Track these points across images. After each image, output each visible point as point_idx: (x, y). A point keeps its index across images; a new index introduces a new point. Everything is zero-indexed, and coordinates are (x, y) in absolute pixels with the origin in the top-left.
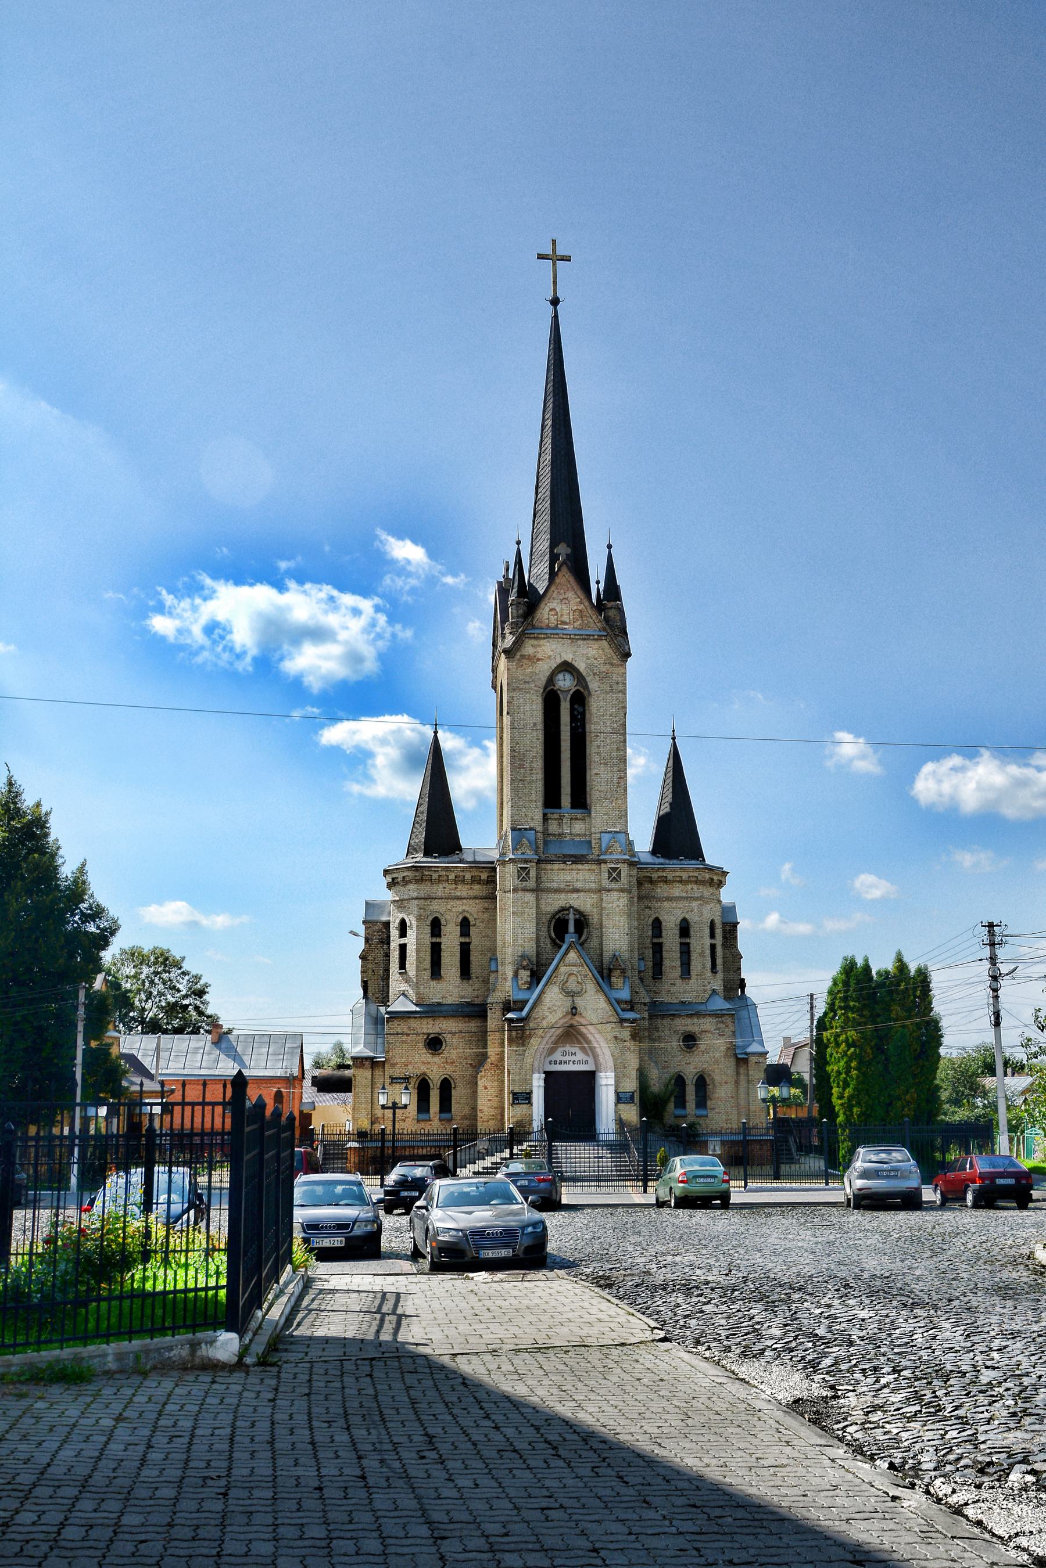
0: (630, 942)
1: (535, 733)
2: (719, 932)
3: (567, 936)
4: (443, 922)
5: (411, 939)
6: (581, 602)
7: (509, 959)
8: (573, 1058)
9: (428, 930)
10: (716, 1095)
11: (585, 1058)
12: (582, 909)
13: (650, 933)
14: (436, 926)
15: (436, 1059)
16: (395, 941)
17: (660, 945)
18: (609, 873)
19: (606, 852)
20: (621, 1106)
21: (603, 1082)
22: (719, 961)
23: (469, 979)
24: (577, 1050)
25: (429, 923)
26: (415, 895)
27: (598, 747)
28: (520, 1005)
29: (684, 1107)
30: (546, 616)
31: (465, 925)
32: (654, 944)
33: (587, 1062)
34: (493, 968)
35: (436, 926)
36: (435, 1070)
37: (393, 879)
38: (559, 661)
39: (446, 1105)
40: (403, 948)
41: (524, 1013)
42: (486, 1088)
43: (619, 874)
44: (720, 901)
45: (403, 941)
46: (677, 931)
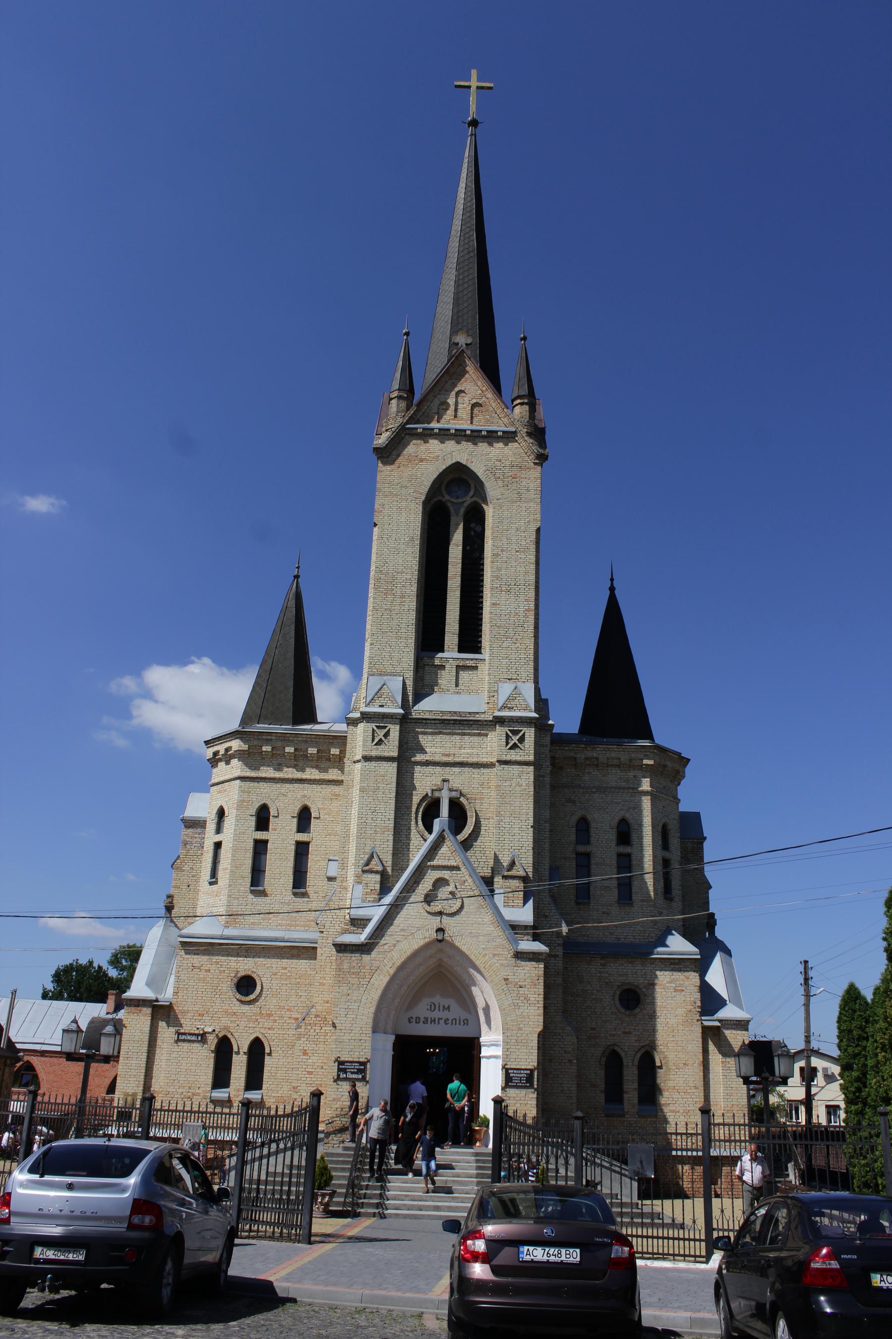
0: (537, 842)
1: (410, 550)
2: (675, 842)
3: (437, 822)
4: (273, 812)
5: (227, 837)
6: (483, 394)
7: (352, 860)
8: (444, 1015)
9: (252, 822)
10: (671, 1084)
11: (464, 1015)
12: (464, 791)
13: (573, 837)
14: (263, 819)
15: (246, 1008)
16: (211, 838)
17: (588, 855)
18: (507, 736)
19: (504, 707)
20: (512, 1092)
21: (484, 1052)
22: (676, 884)
23: (305, 895)
24: (451, 1002)
25: (253, 812)
26: (238, 773)
27: (499, 569)
28: (358, 923)
29: (620, 1101)
30: (435, 410)
31: (304, 818)
32: (578, 854)
33: (466, 1022)
34: (331, 874)
35: (263, 819)
36: (243, 1024)
37: (216, 754)
38: (449, 462)
39: (254, 1080)
40: (218, 845)
41: (362, 937)
42: (305, 1053)
43: (522, 740)
44: (677, 801)
45: (218, 838)
46: (613, 836)
